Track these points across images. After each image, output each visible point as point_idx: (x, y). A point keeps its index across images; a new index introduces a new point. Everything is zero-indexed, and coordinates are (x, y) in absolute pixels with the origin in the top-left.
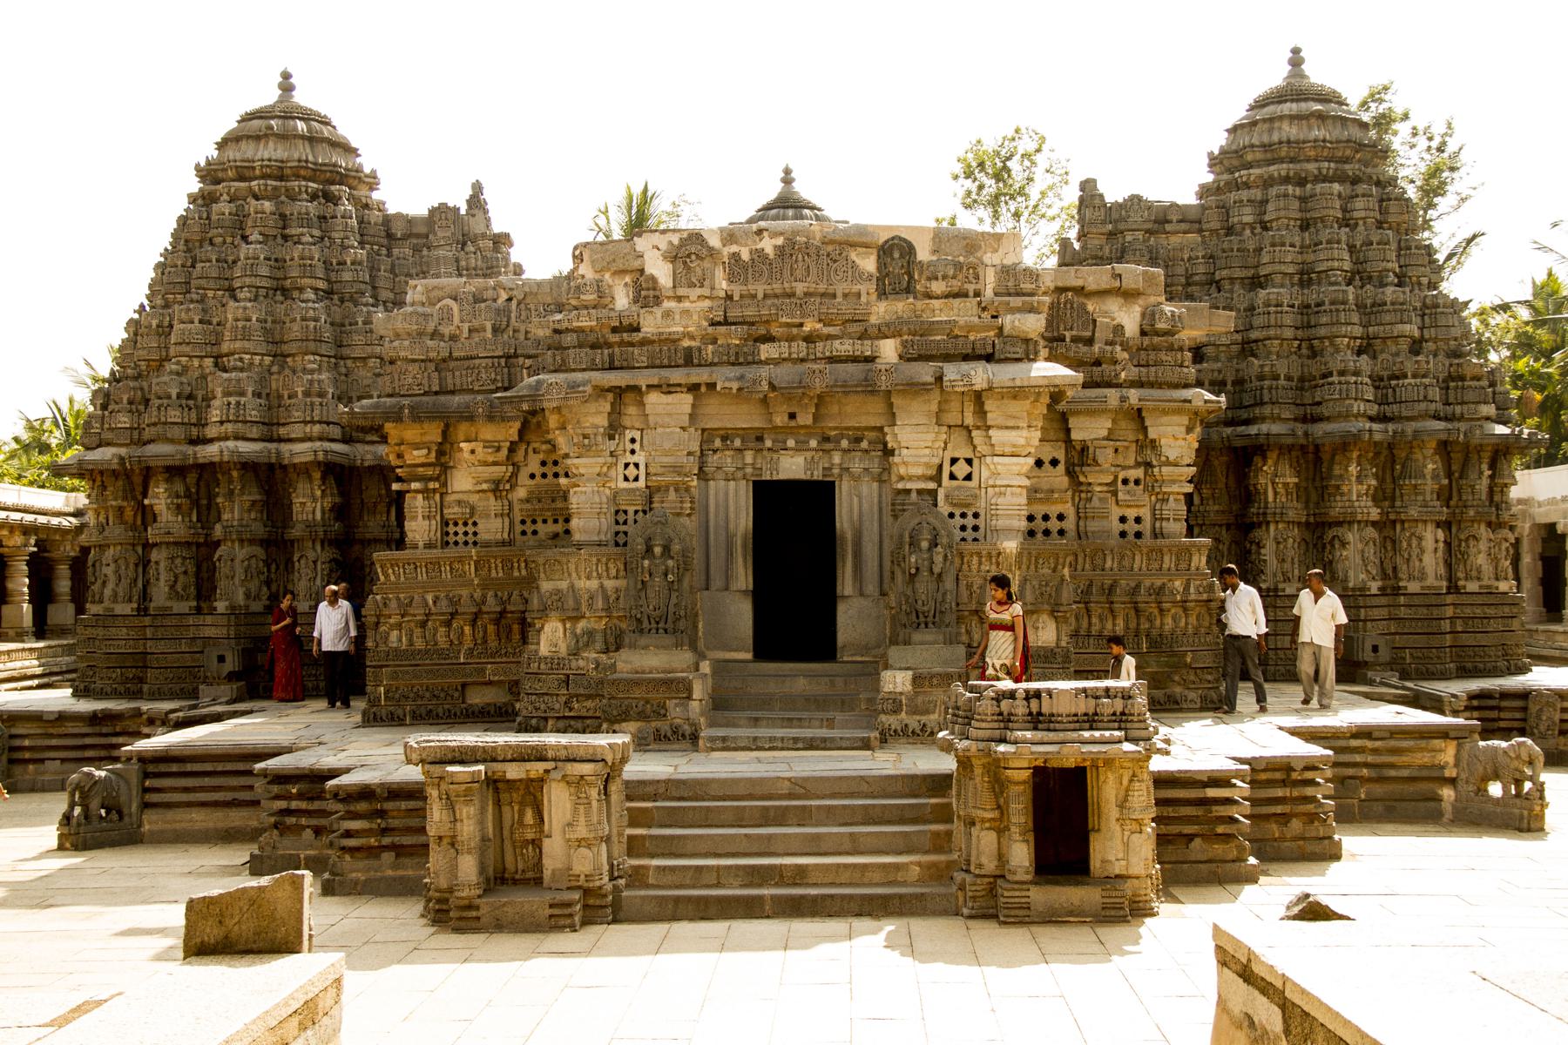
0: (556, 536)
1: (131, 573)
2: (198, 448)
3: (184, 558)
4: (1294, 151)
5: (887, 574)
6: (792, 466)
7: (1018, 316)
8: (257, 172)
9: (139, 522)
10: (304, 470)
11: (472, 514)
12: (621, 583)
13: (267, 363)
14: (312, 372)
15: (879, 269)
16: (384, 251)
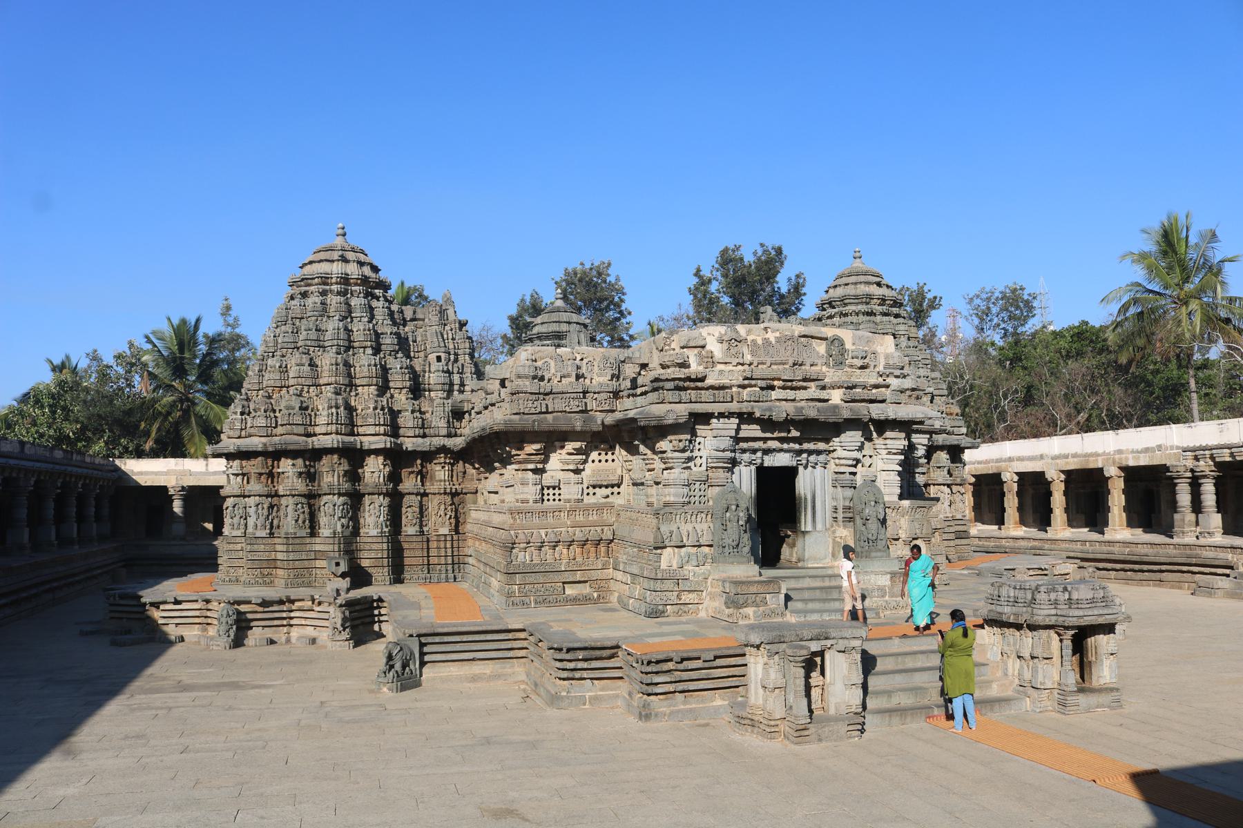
0: (608, 497)
1: (265, 512)
2: (314, 438)
3: (303, 504)
4: (869, 297)
5: (829, 520)
6: (782, 460)
7: (900, 380)
8: (334, 280)
9: (269, 482)
10: (377, 452)
11: (559, 484)
12: (705, 526)
13: (348, 390)
14: (378, 396)
15: (827, 352)
16: (401, 327)
